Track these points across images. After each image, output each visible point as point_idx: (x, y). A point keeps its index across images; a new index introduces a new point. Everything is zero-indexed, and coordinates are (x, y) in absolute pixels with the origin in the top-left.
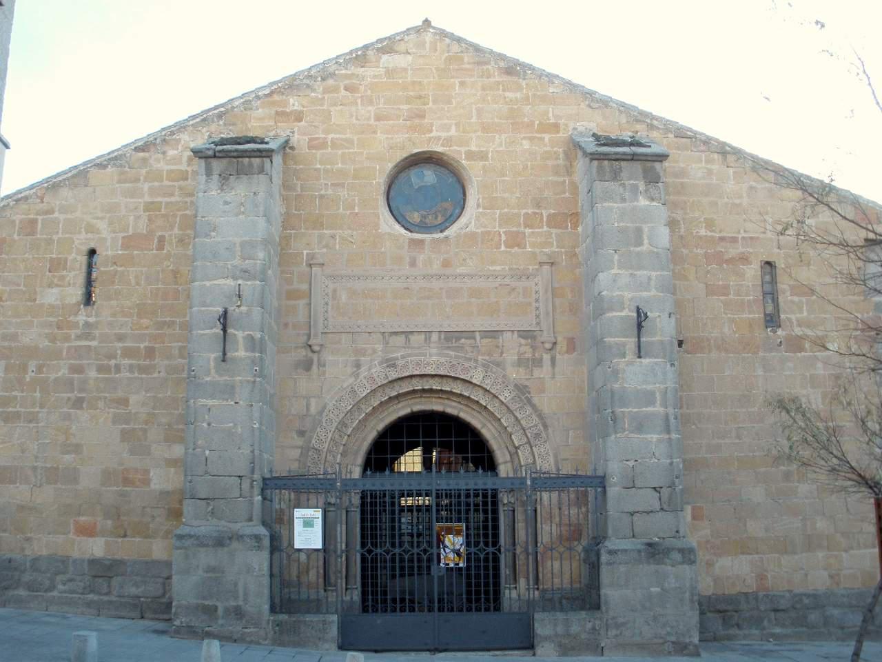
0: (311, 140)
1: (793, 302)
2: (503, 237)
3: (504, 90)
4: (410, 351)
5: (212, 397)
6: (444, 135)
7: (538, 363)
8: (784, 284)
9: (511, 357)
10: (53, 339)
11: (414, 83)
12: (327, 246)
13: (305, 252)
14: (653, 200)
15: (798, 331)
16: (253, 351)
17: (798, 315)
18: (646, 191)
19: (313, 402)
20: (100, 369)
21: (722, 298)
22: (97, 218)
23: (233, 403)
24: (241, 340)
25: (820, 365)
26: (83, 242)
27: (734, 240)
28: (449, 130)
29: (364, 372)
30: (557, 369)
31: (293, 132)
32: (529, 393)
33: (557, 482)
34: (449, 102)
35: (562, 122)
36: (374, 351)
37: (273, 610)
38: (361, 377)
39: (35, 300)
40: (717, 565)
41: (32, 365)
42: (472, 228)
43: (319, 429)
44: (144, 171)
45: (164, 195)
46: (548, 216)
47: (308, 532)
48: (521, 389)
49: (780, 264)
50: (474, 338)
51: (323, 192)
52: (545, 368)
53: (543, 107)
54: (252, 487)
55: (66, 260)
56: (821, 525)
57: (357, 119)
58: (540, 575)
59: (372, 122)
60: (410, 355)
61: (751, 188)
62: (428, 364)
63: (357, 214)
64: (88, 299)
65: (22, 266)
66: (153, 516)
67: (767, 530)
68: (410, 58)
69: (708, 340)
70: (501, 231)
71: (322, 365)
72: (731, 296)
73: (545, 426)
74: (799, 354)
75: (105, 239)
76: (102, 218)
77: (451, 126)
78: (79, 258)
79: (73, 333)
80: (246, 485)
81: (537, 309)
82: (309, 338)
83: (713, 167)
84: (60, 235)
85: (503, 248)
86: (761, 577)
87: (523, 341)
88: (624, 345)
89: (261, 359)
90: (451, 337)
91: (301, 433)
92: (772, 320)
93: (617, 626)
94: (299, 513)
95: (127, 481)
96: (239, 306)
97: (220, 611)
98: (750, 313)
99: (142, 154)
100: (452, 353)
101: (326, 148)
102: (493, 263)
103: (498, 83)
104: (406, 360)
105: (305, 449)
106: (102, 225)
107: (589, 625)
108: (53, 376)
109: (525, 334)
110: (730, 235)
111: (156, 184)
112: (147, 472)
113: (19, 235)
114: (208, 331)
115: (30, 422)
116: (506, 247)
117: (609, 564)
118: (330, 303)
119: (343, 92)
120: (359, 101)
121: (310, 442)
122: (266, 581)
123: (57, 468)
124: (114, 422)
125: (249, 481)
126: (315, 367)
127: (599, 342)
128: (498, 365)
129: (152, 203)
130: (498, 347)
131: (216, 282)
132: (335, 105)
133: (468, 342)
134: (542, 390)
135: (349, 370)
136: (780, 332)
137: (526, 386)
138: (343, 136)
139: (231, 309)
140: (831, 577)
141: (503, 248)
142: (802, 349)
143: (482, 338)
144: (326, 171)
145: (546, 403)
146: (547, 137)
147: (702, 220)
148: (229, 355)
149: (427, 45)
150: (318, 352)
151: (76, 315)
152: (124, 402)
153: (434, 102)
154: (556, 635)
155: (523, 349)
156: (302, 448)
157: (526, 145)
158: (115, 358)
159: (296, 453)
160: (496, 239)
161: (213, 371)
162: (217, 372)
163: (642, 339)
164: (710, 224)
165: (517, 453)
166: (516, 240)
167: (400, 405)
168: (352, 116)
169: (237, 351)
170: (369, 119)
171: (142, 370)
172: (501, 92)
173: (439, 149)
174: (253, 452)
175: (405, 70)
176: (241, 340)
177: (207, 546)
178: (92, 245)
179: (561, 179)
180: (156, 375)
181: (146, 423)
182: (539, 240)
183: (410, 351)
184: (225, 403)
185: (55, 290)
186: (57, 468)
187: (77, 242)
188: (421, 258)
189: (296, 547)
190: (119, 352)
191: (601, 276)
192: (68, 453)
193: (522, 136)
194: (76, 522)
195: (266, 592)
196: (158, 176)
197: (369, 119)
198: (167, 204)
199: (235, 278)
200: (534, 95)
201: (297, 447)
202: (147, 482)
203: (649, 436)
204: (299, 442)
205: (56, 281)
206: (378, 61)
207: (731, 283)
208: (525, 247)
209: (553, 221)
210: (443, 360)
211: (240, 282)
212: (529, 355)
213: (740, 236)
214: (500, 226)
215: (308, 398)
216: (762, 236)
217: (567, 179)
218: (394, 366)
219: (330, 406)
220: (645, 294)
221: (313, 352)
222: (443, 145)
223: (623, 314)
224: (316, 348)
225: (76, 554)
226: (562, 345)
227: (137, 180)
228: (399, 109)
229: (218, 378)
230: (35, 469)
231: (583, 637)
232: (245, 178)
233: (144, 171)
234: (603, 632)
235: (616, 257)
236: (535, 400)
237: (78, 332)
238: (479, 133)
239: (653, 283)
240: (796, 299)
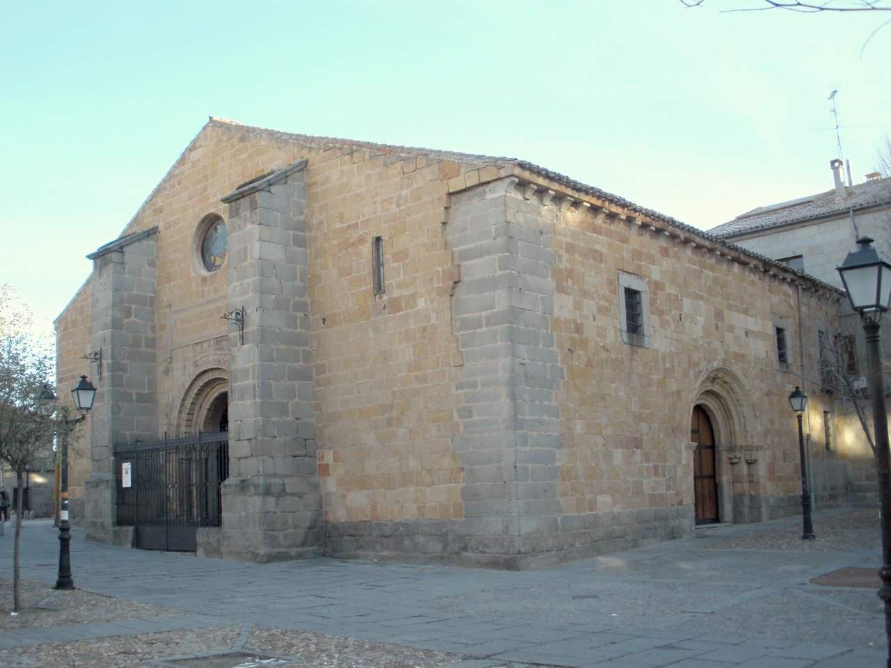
15: (396, 293)
21: (348, 277)
27: (356, 225)
49: (385, 238)
56: (413, 463)
72: (353, 275)
74: (397, 314)
92: (379, 288)
98: (365, 285)
136: (385, 297)
139: (103, 347)
142: (399, 309)
147: (337, 215)
164: (341, 218)
203: (246, 401)
207: (354, 264)
213: (359, 221)
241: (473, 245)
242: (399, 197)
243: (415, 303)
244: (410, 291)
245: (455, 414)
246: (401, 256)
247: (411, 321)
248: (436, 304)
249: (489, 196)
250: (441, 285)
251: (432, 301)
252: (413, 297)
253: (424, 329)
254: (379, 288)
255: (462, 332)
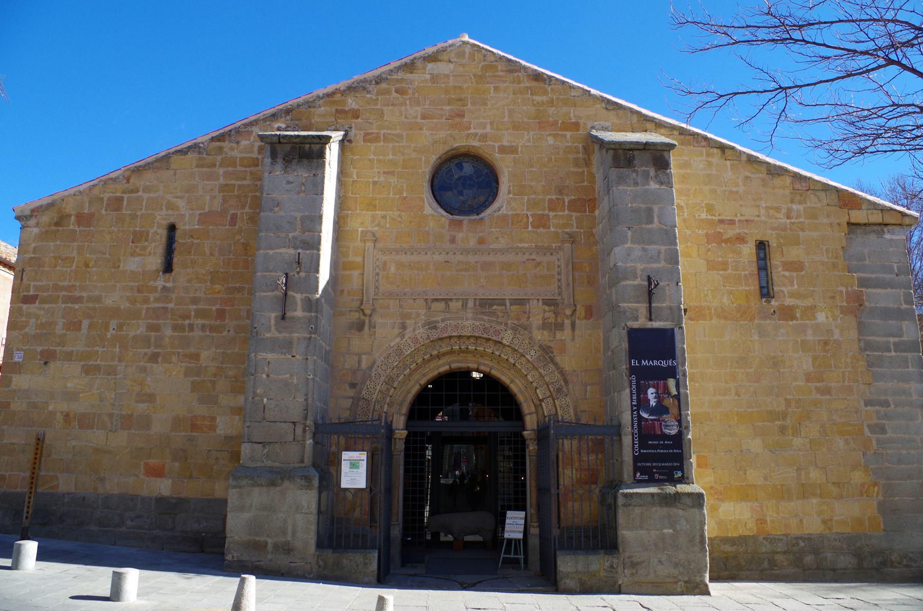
0: (366, 135)
1: (784, 276)
2: (531, 219)
3: (532, 94)
4: (448, 315)
5: (272, 351)
6: (480, 132)
7: (560, 327)
8: (776, 260)
9: (536, 321)
10: (133, 301)
11: (455, 87)
12: (378, 225)
13: (360, 229)
14: (662, 184)
15: (789, 302)
16: (310, 311)
17: (789, 288)
18: (656, 176)
19: (364, 357)
20: (175, 328)
21: (721, 272)
22: (177, 197)
23: (290, 356)
24: (299, 302)
25: (810, 332)
26: (162, 218)
27: (732, 222)
28: (485, 128)
29: (408, 334)
30: (577, 332)
31: (351, 128)
32: (552, 353)
33: (576, 429)
34: (486, 104)
35: (582, 121)
36: (418, 315)
37: (320, 545)
38: (406, 337)
39: (119, 267)
40: (721, 510)
41: (113, 324)
42: (503, 211)
43: (368, 383)
44: (219, 158)
45: (237, 179)
46: (569, 202)
47: (354, 472)
48: (546, 351)
49: (773, 244)
50: (505, 305)
51: (376, 179)
52: (566, 332)
53: (565, 109)
54: (304, 431)
55: (148, 233)
56: (815, 475)
57: (406, 117)
58: (562, 515)
59: (419, 120)
60: (449, 319)
61: (747, 177)
62: (465, 326)
63: (405, 198)
64: (168, 267)
65: (108, 237)
66: (217, 459)
67: (765, 478)
68: (452, 66)
69: (709, 309)
70: (529, 213)
71: (372, 326)
72: (729, 271)
73: (566, 382)
75: (184, 215)
76: (181, 198)
77: (486, 124)
78: (159, 231)
79: (152, 297)
80: (299, 430)
81: (559, 280)
82: (362, 304)
83: (713, 160)
84: (143, 211)
85: (530, 228)
86: (761, 521)
87: (547, 308)
88: (637, 310)
89: (317, 317)
90: (485, 304)
91: (353, 385)
92: (766, 292)
93: (634, 565)
94: (346, 455)
95: (194, 427)
96: (298, 273)
97: (270, 547)
98: (746, 285)
99: (218, 144)
100: (486, 318)
101: (379, 142)
102: (521, 241)
103: (527, 88)
104: (445, 323)
105: (356, 400)
106: (181, 203)
107: (607, 564)
108: (132, 334)
109: (547, 302)
110: (729, 218)
111: (230, 169)
112: (213, 419)
113: (106, 210)
114: (268, 294)
115: (109, 374)
116: (533, 227)
117: (624, 505)
118: (381, 273)
119: (394, 94)
120: (408, 102)
121: (361, 393)
122: (313, 518)
123: (132, 415)
124: (186, 375)
125: (302, 426)
126: (366, 328)
127: (614, 308)
128: (525, 328)
129: (227, 185)
130: (525, 313)
131: (278, 251)
132: (388, 105)
133: (499, 308)
134: (563, 351)
135: (397, 331)
136: (773, 302)
137: (550, 347)
138: (393, 132)
140: (824, 522)
141: (530, 228)
142: (793, 318)
143: (511, 305)
144: (379, 161)
145: (567, 362)
146: (568, 134)
148: (288, 314)
149: (467, 55)
150: (370, 316)
151: (155, 280)
152: (196, 357)
153: (473, 103)
154: (577, 572)
155: (547, 315)
156: (353, 398)
157: (551, 140)
158: (189, 317)
159: (348, 403)
160: (525, 220)
161: (273, 328)
162: (276, 329)
163: (653, 305)
165: (541, 405)
166: (541, 222)
167: (441, 362)
168: (401, 115)
169: (295, 310)
170: (416, 117)
171: (213, 329)
172: (529, 96)
173: (476, 143)
174: (306, 400)
175: (447, 76)
176: (299, 302)
177: (261, 485)
178: (172, 220)
179: (581, 170)
180: (225, 333)
181: (215, 375)
182: (561, 222)
183: (448, 315)
184: (283, 356)
185: (137, 259)
186: (132, 415)
187: (158, 217)
188: (460, 236)
189: (342, 486)
190: (193, 313)
191: (617, 250)
192: (143, 401)
193: (548, 133)
194: (146, 464)
195: (313, 528)
196: (232, 162)
197: (416, 117)
198: (239, 186)
199: (295, 248)
200: (557, 99)
201: (349, 398)
202: (213, 428)
204: (351, 393)
205: (138, 250)
206: (424, 68)
208: (549, 228)
209: (575, 206)
210: (477, 323)
211: (300, 251)
212: (552, 320)
214: (528, 210)
215: (359, 355)
216: (756, 219)
217: (585, 169)
218: (435, 328)
219: (379, 363)
220: (655, 265)
221: (365, 315)
222: (479, 140)
223: (636, 283)
224: (368, 312)
225: (145, 493)
226: (581, 311)
227: (214, 165)
228: (442, 109)
229: (277, 335)
230: (111, 415)
231: (602, 574)
232: (305, 161)
233: (219, 158)
234: (620, 570)
235: (630, 233)
236: (558, 359)
237: (157, 295)
238: (511, 131)
239: (662, 256)
240: (787, 274)
241: (873, 276)
242: (789, 211)
243: (814, 316)
244: (808, 302)
245: (866, 430)
246: (795, 266)
247: (810, 332)
248: (839, 321)
249: (888, 236)
250: (845, 304)
251: (835, 318)
252: (813, 308)
253: (826, 343)
254: (766, 292)
255: (867, 353)
